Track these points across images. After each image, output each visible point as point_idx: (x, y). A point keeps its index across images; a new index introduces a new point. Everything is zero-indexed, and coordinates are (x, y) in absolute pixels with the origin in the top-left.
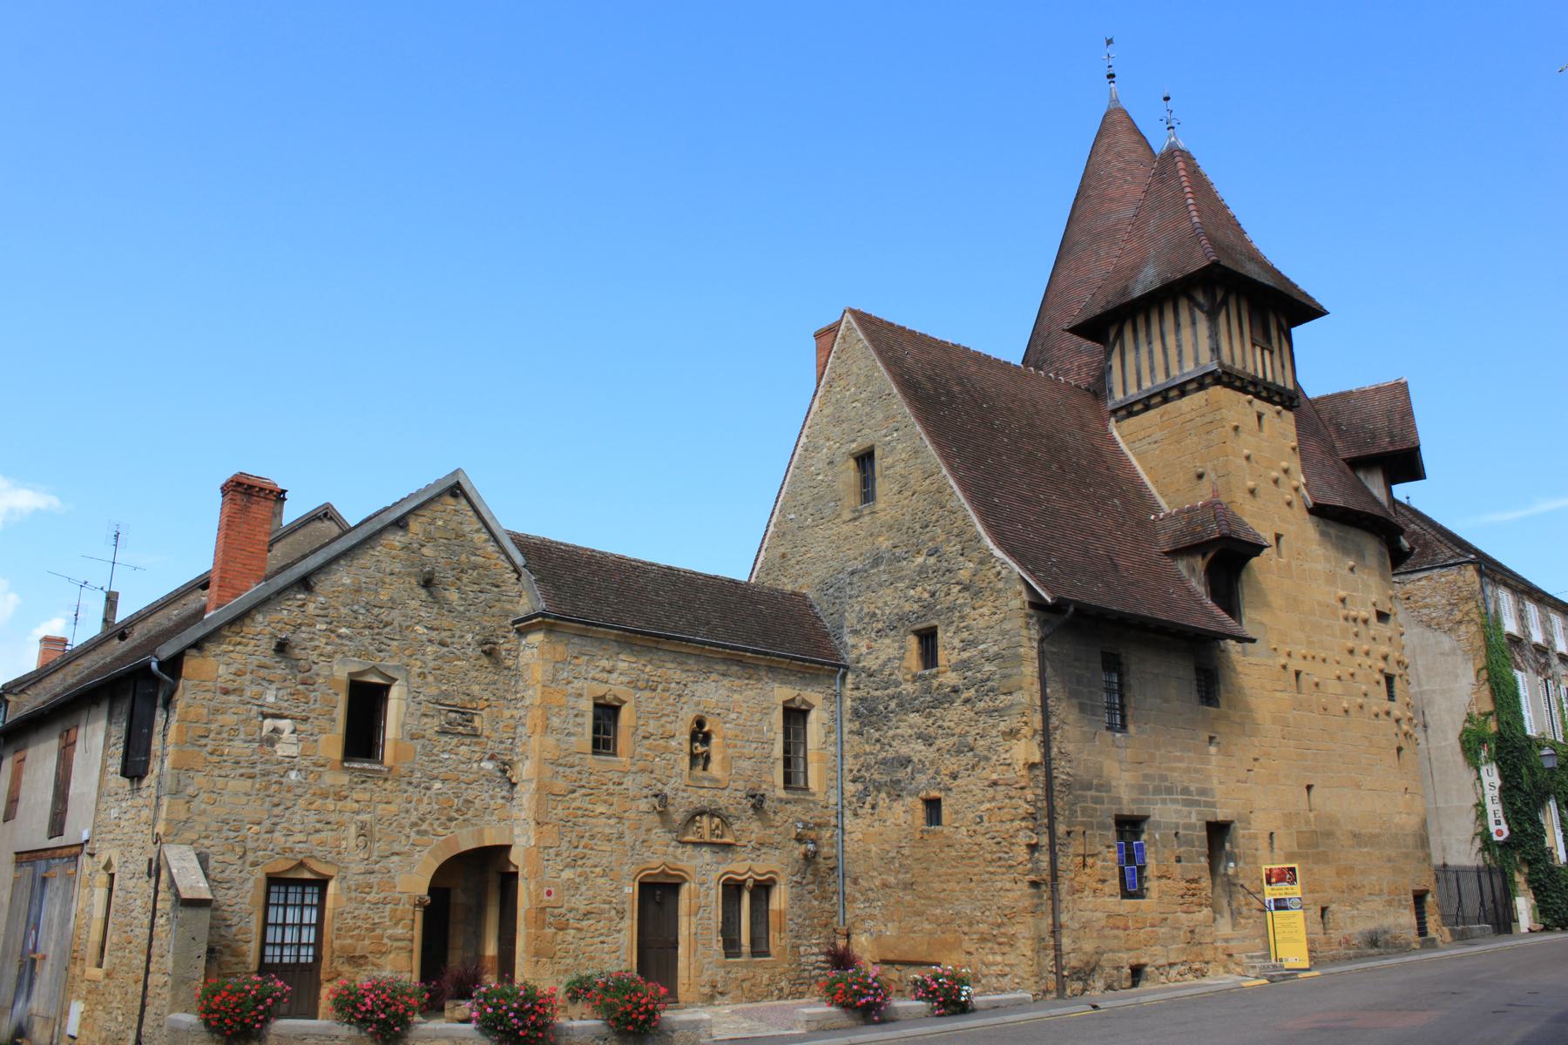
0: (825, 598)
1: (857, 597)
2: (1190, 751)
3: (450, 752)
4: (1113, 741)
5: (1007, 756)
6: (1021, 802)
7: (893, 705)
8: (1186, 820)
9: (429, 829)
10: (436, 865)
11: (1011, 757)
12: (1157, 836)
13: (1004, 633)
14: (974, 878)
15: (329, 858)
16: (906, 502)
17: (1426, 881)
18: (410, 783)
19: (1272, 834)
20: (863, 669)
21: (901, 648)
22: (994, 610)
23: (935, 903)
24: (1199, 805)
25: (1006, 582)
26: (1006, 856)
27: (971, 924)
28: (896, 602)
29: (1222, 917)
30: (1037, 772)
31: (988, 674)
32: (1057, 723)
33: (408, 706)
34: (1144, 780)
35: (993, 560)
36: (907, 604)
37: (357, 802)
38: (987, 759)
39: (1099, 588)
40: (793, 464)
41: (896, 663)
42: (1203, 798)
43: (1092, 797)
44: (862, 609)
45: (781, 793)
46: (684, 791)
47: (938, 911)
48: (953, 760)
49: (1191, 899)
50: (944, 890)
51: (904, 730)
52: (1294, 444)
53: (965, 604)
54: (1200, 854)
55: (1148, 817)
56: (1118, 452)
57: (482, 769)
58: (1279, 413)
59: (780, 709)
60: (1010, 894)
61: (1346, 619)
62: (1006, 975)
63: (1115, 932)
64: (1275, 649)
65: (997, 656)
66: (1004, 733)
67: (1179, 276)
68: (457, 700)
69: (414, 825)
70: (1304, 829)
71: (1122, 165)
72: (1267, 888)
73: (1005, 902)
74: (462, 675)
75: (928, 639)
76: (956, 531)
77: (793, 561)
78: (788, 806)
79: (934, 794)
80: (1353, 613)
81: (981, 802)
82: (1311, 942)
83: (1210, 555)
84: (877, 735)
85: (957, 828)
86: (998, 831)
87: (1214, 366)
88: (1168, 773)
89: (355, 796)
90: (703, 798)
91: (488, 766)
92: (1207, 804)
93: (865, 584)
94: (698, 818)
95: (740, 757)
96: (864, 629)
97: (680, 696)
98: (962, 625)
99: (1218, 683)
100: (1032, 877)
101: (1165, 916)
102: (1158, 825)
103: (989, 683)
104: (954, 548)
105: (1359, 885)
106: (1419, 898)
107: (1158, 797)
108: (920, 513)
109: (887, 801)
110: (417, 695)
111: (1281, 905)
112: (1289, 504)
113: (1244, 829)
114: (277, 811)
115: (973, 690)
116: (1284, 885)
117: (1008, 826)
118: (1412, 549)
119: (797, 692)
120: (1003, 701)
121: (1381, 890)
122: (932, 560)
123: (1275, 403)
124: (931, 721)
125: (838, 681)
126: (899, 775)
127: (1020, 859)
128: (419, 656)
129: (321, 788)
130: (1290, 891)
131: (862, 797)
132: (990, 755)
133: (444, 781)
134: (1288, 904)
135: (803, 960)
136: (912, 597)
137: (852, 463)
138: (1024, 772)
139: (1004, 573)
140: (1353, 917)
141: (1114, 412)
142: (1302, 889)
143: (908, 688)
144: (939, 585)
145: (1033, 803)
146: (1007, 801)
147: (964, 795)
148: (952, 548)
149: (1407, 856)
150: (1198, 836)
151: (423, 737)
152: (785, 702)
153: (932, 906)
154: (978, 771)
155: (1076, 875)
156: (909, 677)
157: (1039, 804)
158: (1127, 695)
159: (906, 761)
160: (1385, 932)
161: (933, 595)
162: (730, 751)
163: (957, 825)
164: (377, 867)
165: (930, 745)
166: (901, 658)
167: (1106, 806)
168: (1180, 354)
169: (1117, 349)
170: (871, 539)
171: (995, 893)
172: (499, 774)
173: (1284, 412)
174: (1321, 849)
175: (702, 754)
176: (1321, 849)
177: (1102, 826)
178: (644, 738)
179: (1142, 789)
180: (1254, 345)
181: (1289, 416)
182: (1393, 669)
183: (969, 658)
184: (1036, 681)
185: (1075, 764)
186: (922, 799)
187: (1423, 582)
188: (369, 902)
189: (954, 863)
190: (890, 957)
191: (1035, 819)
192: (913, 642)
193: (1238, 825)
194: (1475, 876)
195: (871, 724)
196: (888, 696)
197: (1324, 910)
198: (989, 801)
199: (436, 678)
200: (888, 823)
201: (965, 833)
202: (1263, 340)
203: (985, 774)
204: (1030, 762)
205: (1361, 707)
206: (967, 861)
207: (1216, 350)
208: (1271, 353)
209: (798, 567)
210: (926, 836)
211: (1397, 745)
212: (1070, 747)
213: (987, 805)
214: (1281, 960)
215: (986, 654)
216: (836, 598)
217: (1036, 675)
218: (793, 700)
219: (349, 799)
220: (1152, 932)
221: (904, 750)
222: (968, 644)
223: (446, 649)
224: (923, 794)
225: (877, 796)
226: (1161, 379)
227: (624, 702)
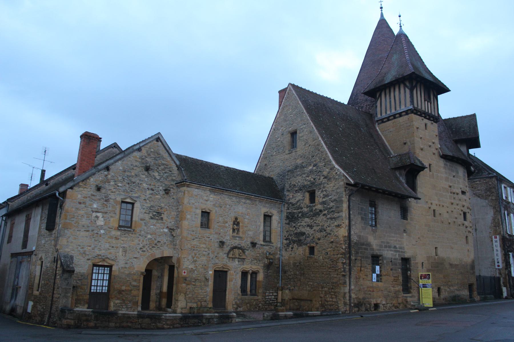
0: (279, 179)
1: (290, 179)
4: (372, 230)
5: (337, 233)
6: (341, 249)
7: (300, 215)
10: (148, 262)
11: (338, 234)
12: (385, 262)
13: (337, 193)
14: (324, 273)
16: (307, 148)
17: (473, 280)
18: (140, 235)
19: (423, 263)
20: (291, 203)
21: (303, 196)
22: (334, 185)
25: (339, 176)
26: (335, 266)
27: (322, 288)
28: (302, 181)
31: (331, 206)
33: (140, 210)
35: (335, 169)
36: (306, 182)
38: (330, 234)
39: (369, 179)
40: (270, 135)
41: (301, 201)
42: (401, 250)
43: (364, 248)
44: (291, 183)
45: (262, 243)
46: (230, 240)
47: (312, 283)
48: (319, 234)
51: (303, 223)
52: (437, 134)
53: (325, 183)
56: (378, 135)
57: (164, 231)
58: (432, 123)
61: (451, 193)
64: (427, 202)
65: (335, 200)
66: (336, 226)
67: (401, 77)
69: (141, 248)
71: (384, 38)
76: (323, 159)
77: (269, 166)
78: (264, 247)
79: (312, 245)
80: (454, 191)
81: (328, 248)
82: (434, 298)
83: (407, 170)
84: (294, 225)
85: (319, 256)
87: (411, 107)
89: (122, 239)
90: (236, 242)
92: (402, 252)
94: (234, 250)
95: (249, 230)
96: (291, 190)
97: (230, 209)
98: (324, 190)
99: (408, 212)
101: (386, 288)
103: (332, 209)
104: (322, 164)
106: (470, 286)
107: (386, 249)
108: (311, 152)
109: (297, 246)
111: (424, 286)
112: (434, 154)
113: (413, 260)
114: (96, 243)
116: (426, 280)
117: (336, 256)
118: (475, 171)
119: (269, 210)
120: (336, 215)
122: (315, 168)
123: (431, 120)
124: (312, 221)
127: (339, 267)
128: (144, 194)
130: (428, 282)
131: (288, 245)
132: (331, 233)
133: (151, 234)
134: (427, 286)
135: (267, 297)
136: (308, 180)
137: (289, 135)
139: (338, 173)
141: (377, 121)
142: (432, 281)
143: (305, 210)
144: (317, 176)
146: (336, 248)
147: (322, 246)
148: (321, 164)
150: (398, 262)
151: (144, 220)
152: (264, 213)
153: (310, 281)
154: (327, 238)
156: (305, 206)
158: (377, 215)
159: (303, 234)
161: (314, 179)
162: (246, 228)
163: (319, 255)
164: (128, 262)
165: (312, 229)
166: (303, 200)
168: (400, 102)
169: (379, 100)
170: (295, 160)
172: (169, 233)
173: (434, 123)
175: (237, 229)
177: (367, 257)
178: (218, 223)
179: (381, 246)
180: (425, 101)
181: (436, 125)
182: (467, 210)
183: (326, 200)
184: (347, 209)
186: (308, 246)
187: (478, 182)
189: (318, 268)
190: (296, 297)
192: (307, 195)
193: (412, 259)
195: (292, 221)
196: (298, 212)
198: (330, 248)
199: (150, 201)
200: (297, 254)
201: (322, 258)
202: (428, 99)
203: (329, 239)
207: (412, 102)
208: (431, 103)
209: (270, 169)
210: (309, 259)
211: (466, 235)
213: (330, 249)
214: (424, 304)
215: (331, 200)
216: (283, 179)
217: (347, 207)
218: (267, 212)
221: (303, 230)
223: (153, 192)
224: (308, 245)
225: (293, 245)
226: (393, 111)
227: (212, 211)
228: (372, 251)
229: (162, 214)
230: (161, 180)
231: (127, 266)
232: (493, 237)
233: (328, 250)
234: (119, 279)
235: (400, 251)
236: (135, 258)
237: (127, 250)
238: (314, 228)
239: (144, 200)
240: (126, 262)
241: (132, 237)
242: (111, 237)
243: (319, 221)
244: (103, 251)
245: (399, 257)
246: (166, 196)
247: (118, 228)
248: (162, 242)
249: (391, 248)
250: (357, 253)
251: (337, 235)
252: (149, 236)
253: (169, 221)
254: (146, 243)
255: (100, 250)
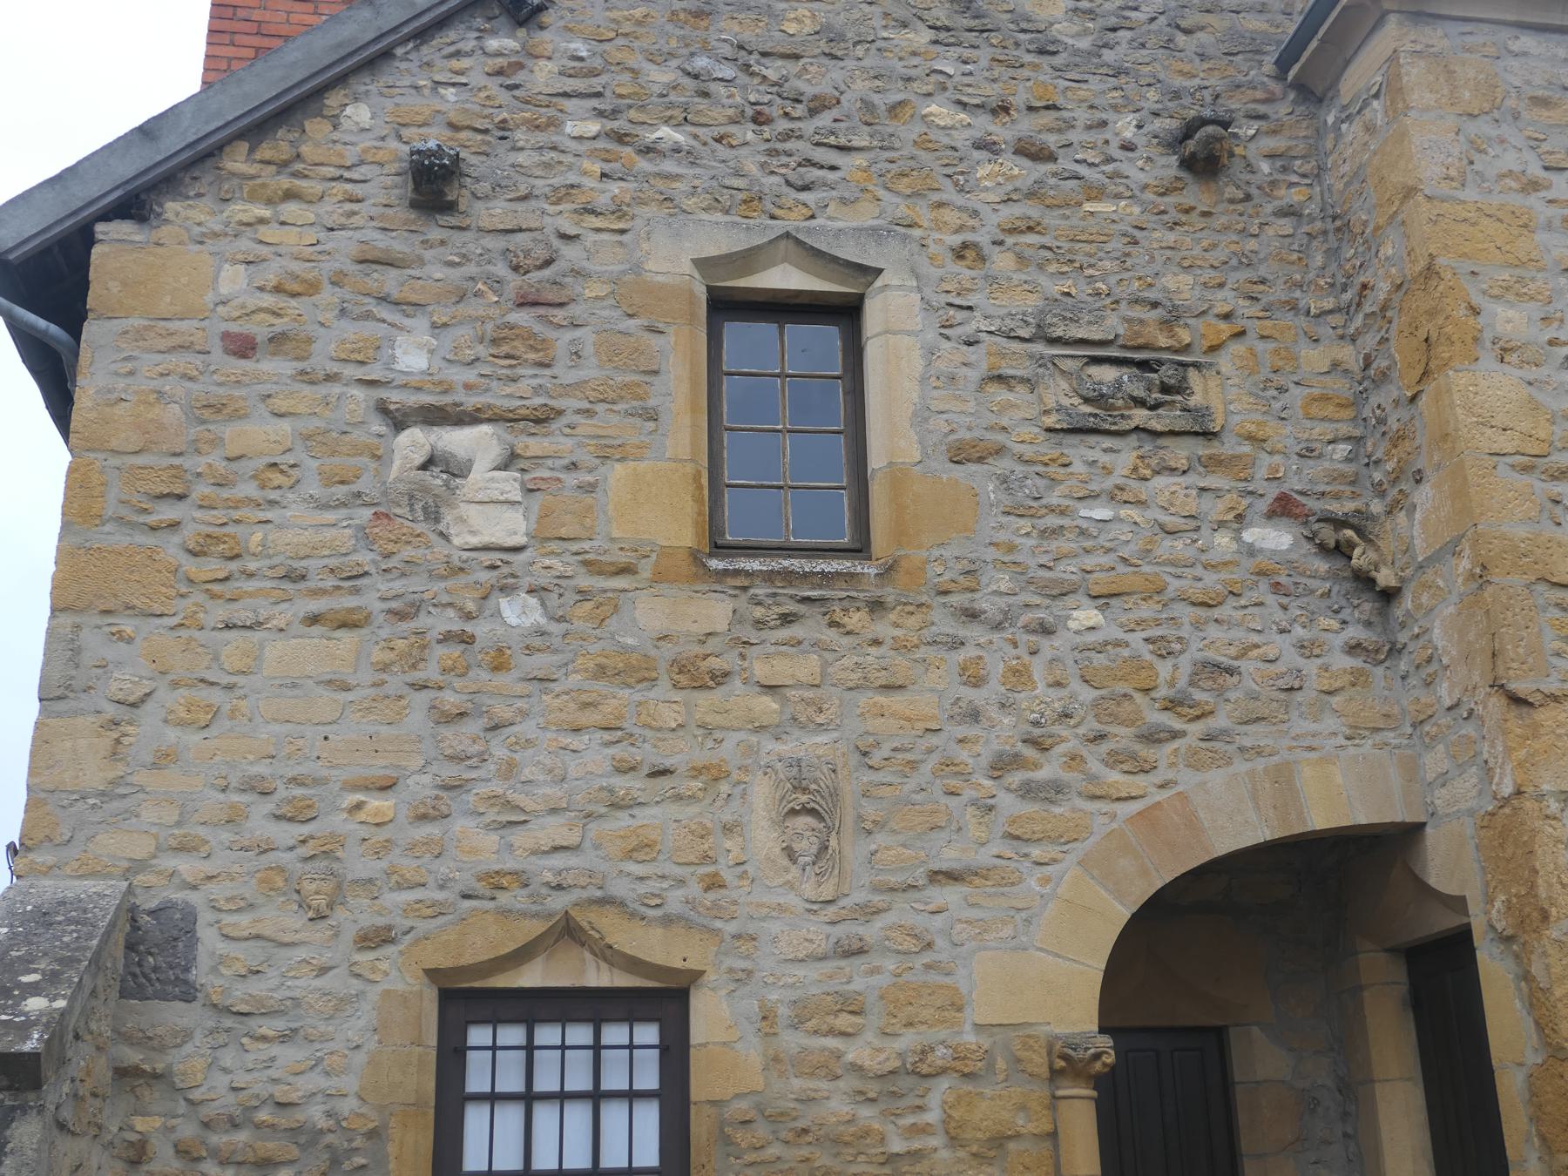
3: (1115, 496)
9: (1067, 776)
15: (675, 901)
18: (972, 615)
33: (930, 352)
37: (771, 689)
57: (1252, 551)
68: (1113, 325)
69: (1001, 766)
74: (1117, 245)
89: (760, 671)
91: (1277, 538)
110: (960, 316)
114: (462, 737)
128: (950, 194)
129: (625, 650)
133: (1103, 599)
151: (1000, 451)
164: (871, 932)
172: (1322, 565)
188: (857, 1069)
199: (1021, 259)
219: (738, 683)
223: (1050, 167)
229: (1192, 374)
230: (1108, 56)
231: (859, 979)
234: (774, 1151)
236: (953, 877)
237: (834, 794)
239: (959, 253)
240: (839, 931)
241: (876, 642)
242: (636, 672)
244: (553, 830)
246: (1195, 195)
247: (695, 556)
248: (1246, 666)
252: (1086, 615)
253: (1285, 435)
254: (1056, 700)
255: (513, 820)
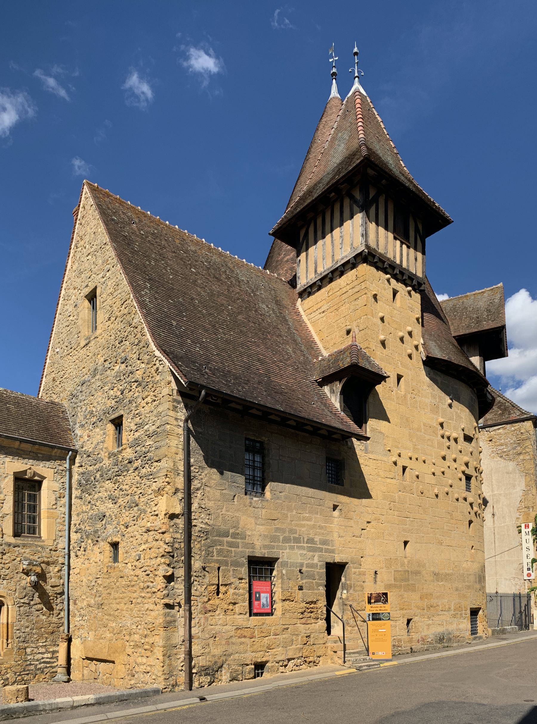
2: (317, 513)
6: (162, 543)
8: (309, 561)
12: (284, 572)
21: (104, 434)
23: (113, 619)
24: (321, 551)
26: (151, 585)
29: (338, 625)
30: (176, 521)
32: (199, 485)
34: (276, 531)
35: (155, 359)
43: (227, 542)
48: (127, 513)
49: (309, 615)
50: (118, 609)
54: (318, 585)
55: (277, 559)
59: (11, 478)
60: (153, 613)
62: (148, 673)
63: (243, 640)
70: (400, 569)
72: (368, 606)
73: (149, 619)
75: (118, 423)
79: (115, 539)
86: (148, 566)
88: (298, 528)
92: (327, 551)
93: (88, 391)
98: (136, 412)
100: (167, 601)
102: (285, 564)
105: (435, 605)
113: (355, 568)
115: (139, 460)
116: (380, 604)
117: (153, 562)
119: (29, 467)
121: (450, 608)
124: (117, 486)
125: (68, 460)
126: (98, 526)
127: (159, 587)
138: (166, 520)
140: (429, 625)
145: (170, 544)
146: (154, 543)
147: (131, 539)
149: (469, 587)
150: (317, 572)
155: (209, 600)
157: (176, 545)
160: (450, 633)
167: (240, 549)
171: (144, 612)
174: (410, 582)
176: (410, 582)
177: (236, 564)
179: (274, 539)
185: (213, 517)
191: (173, 557)
194: (512, 598)
196: (96, 469)
197: (409, 621)
204: (171, 512)
205: (447, 494)
206: (130, 588)
212: (210, 504)
213: (143, 547)
215: (148, 433)
220: (276, 638)
222: (139, 426)
228: (252, 550)
232: (523, 526)
233: (141, 549)
235: (322, 549)
238: (120, 501)
243: (126, 485)
245: (320, 561)
249: (300, 543)
250: (209, 554)
251: (156, 513)
